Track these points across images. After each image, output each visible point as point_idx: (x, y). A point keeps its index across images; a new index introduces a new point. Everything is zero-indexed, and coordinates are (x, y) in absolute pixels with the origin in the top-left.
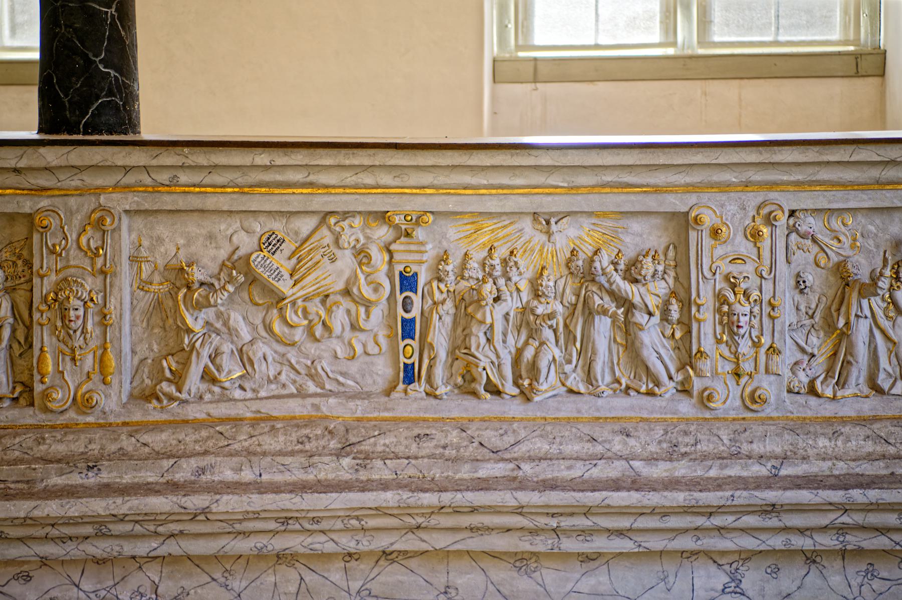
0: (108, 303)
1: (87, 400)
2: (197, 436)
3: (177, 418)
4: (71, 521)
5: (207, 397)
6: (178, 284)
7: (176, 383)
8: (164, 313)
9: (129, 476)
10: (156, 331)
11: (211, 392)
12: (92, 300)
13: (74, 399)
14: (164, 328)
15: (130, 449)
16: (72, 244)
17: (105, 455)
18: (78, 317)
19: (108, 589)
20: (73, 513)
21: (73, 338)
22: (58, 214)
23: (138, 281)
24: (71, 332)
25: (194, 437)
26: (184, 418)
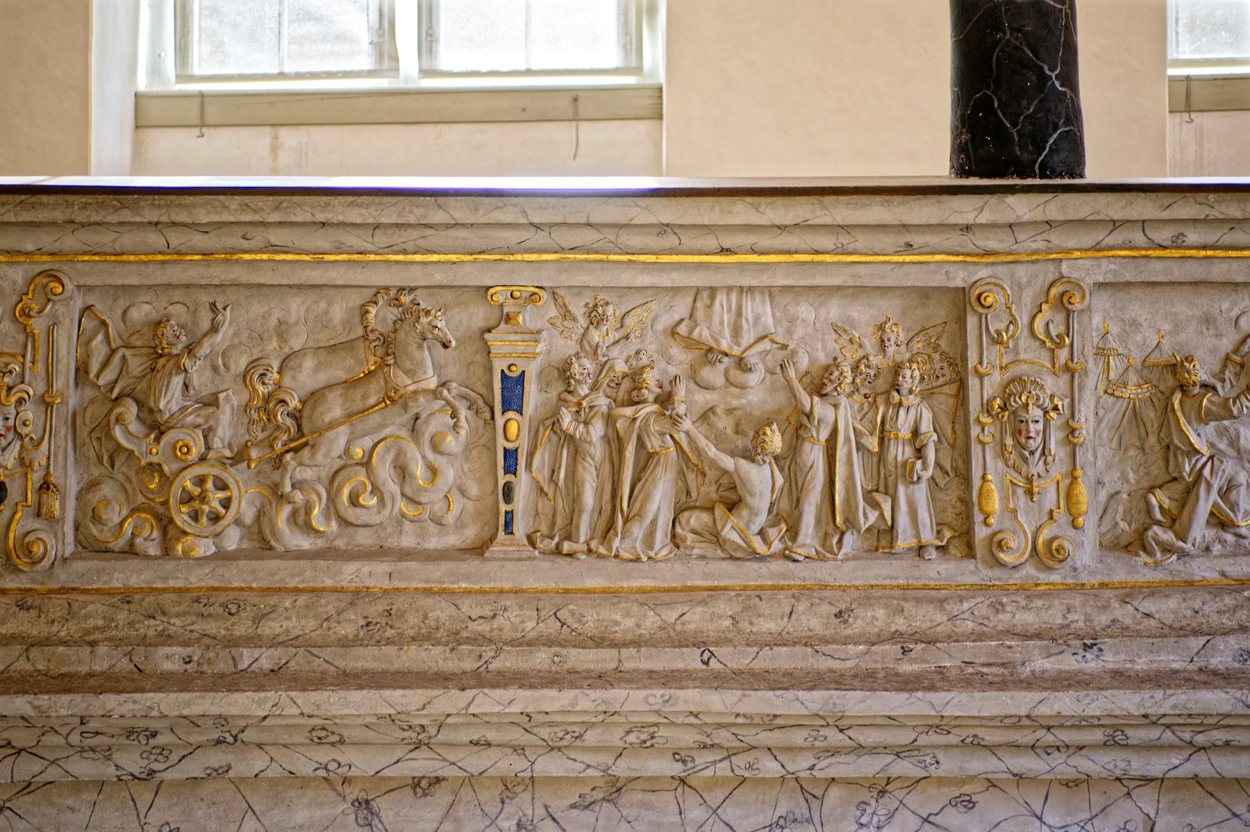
0: (1076, 414)
1: (1057, 550)
2: (1218, 605)
3: (1176, 579)
4: (1084, 723)
5: (1217, 548)
6: (1162, 387)
7: (1171, 527)
8: (1142, 428)
9: (1143, 660)
10: (1132, 453)
11: (1223, 542)
12: (1056, 408)
13: (1034, 548)
14: (1142, 449)
15: (1128, 621)
16: (1022, 331)
17: (1097, 628)
18: (1038, 433)
19: (1082, 824)
20: (1094, 711)
21: (1030, 462)
22: (1003, 289)
23: (1105, 382)
24: (1027, 453)
25: (1215, 606)
26: (1187, 578)
